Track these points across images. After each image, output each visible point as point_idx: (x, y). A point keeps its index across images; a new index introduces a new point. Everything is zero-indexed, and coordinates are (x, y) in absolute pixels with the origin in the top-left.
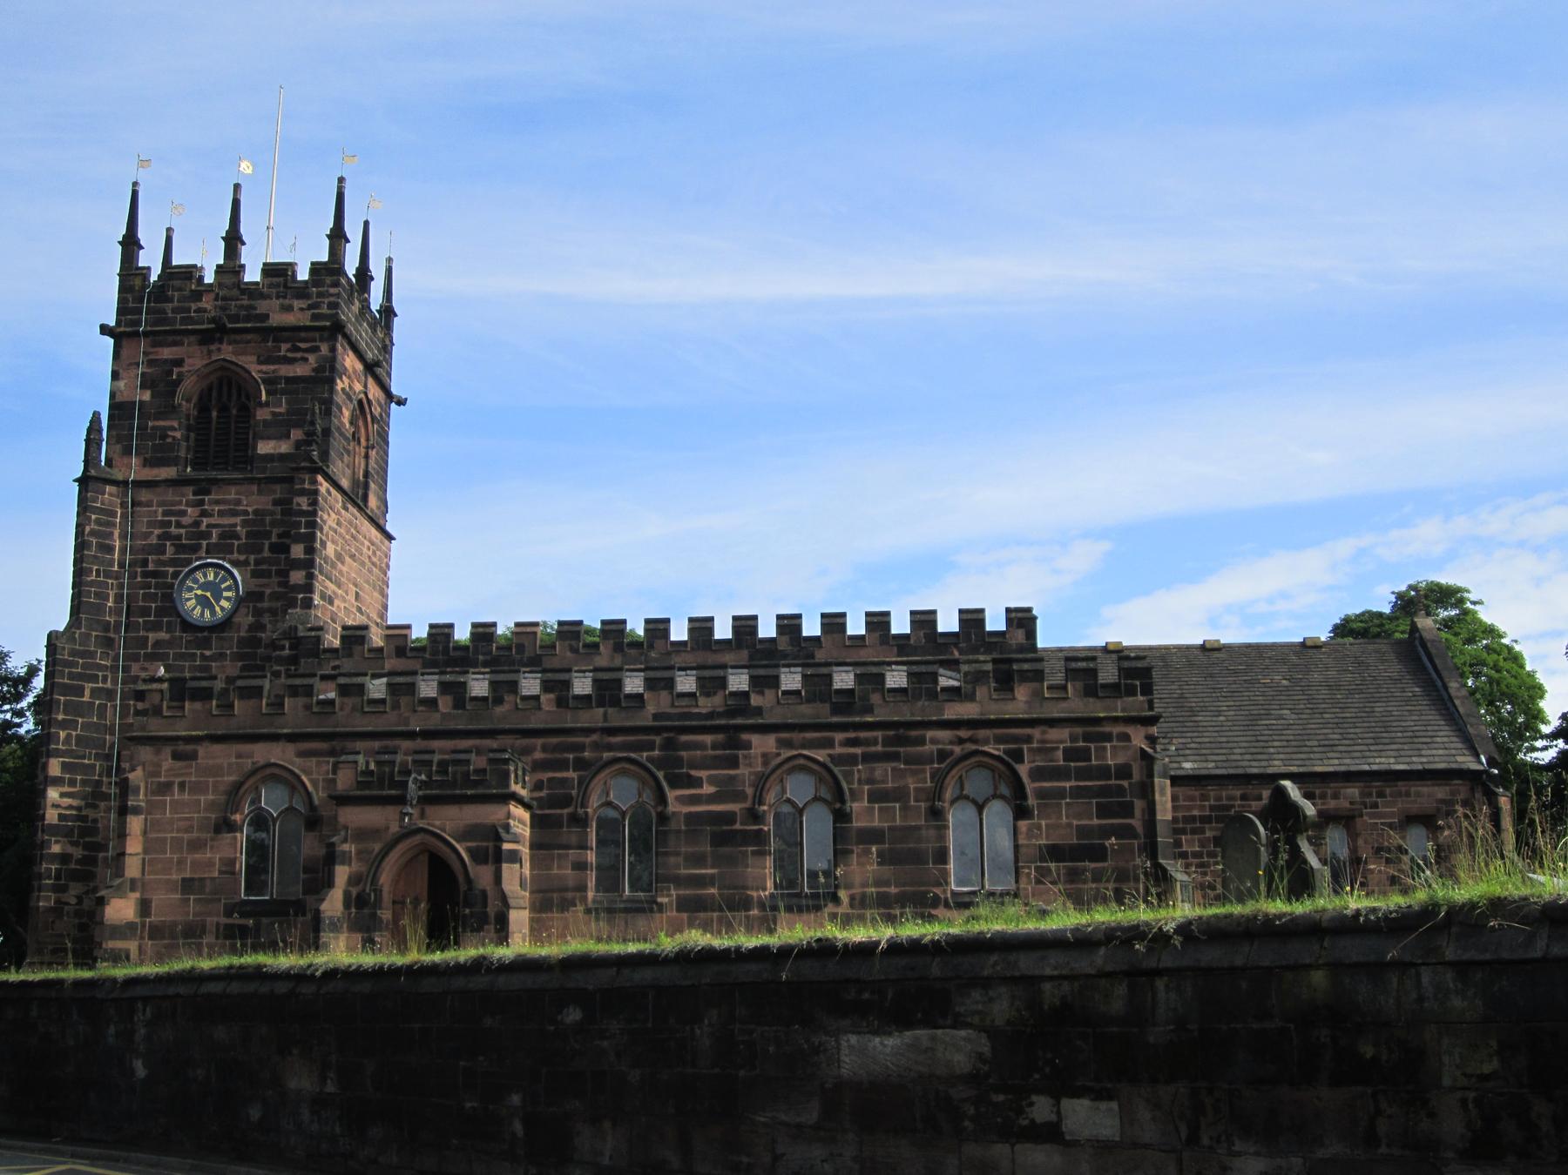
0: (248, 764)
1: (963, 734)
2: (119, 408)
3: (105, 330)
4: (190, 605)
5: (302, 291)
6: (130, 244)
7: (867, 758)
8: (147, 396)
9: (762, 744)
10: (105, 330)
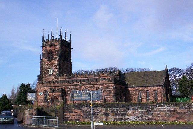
0: (45, 89)
1: (98, 85)
2: (43, 54)
3: (41, 46)
4: (50, 73)
5: (57, 41)
6: (43, 38)
7: (91, 87)
8: (45, 52)
9: (83, 86)
10: (41, 46)
